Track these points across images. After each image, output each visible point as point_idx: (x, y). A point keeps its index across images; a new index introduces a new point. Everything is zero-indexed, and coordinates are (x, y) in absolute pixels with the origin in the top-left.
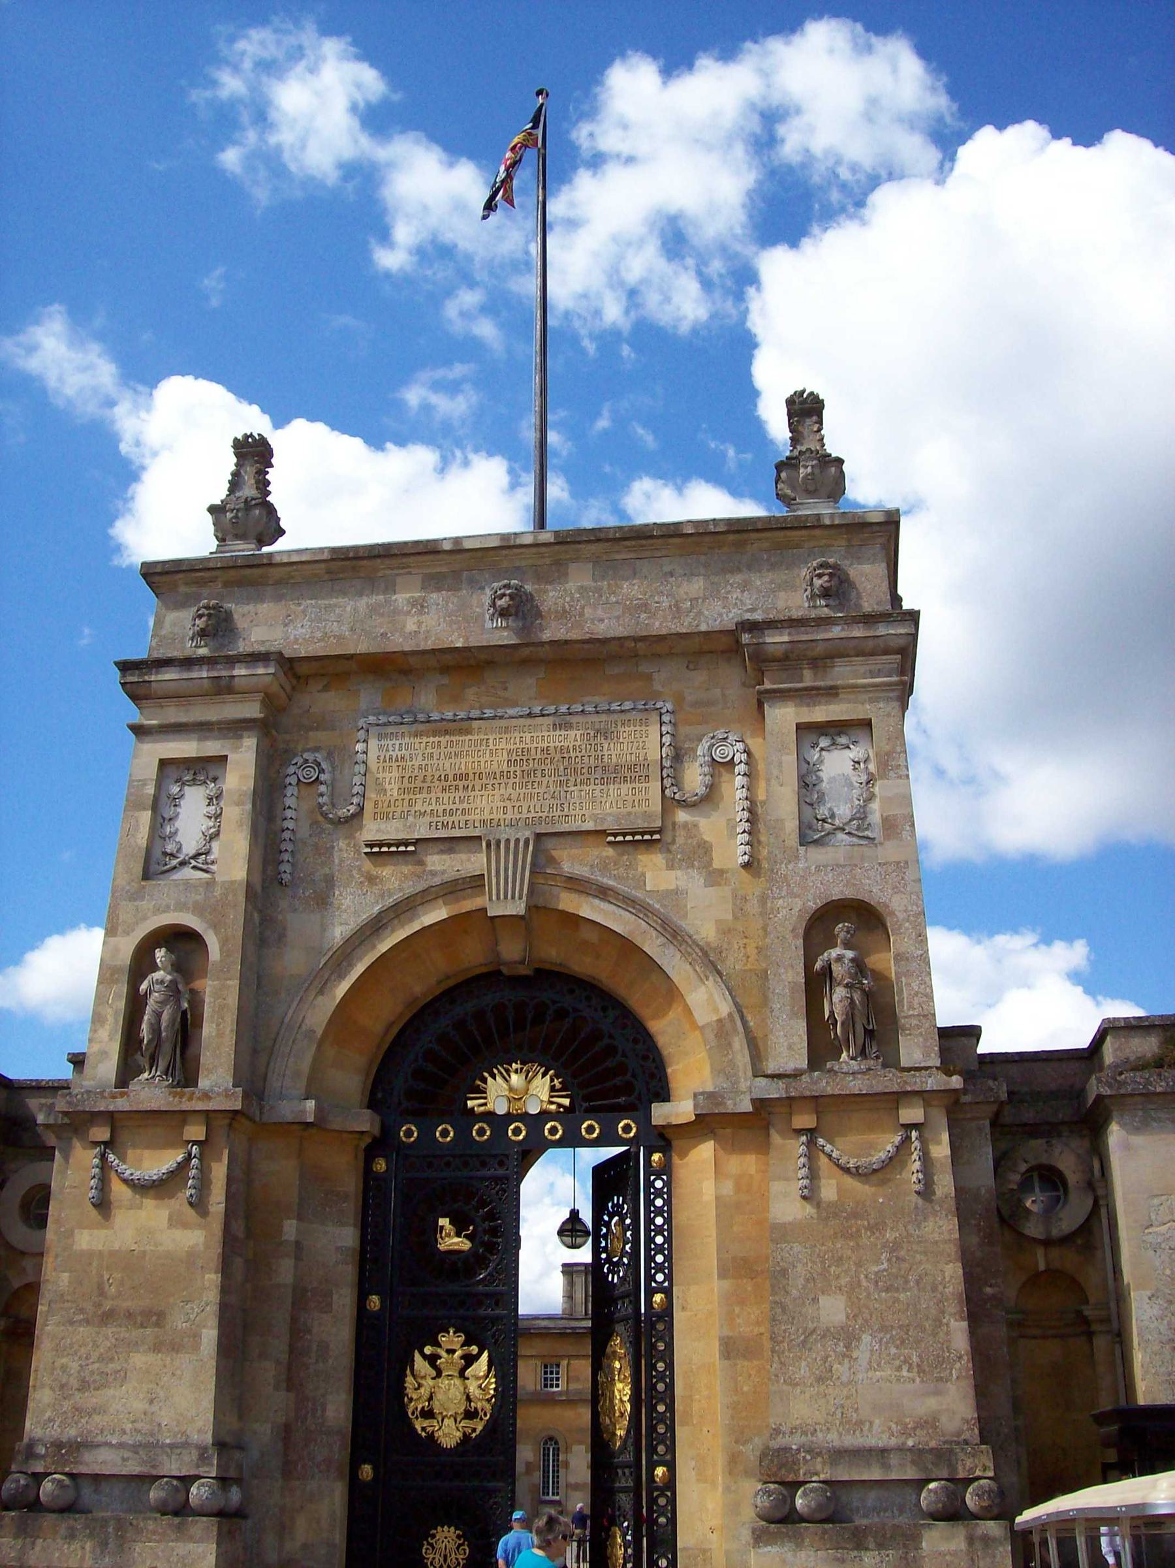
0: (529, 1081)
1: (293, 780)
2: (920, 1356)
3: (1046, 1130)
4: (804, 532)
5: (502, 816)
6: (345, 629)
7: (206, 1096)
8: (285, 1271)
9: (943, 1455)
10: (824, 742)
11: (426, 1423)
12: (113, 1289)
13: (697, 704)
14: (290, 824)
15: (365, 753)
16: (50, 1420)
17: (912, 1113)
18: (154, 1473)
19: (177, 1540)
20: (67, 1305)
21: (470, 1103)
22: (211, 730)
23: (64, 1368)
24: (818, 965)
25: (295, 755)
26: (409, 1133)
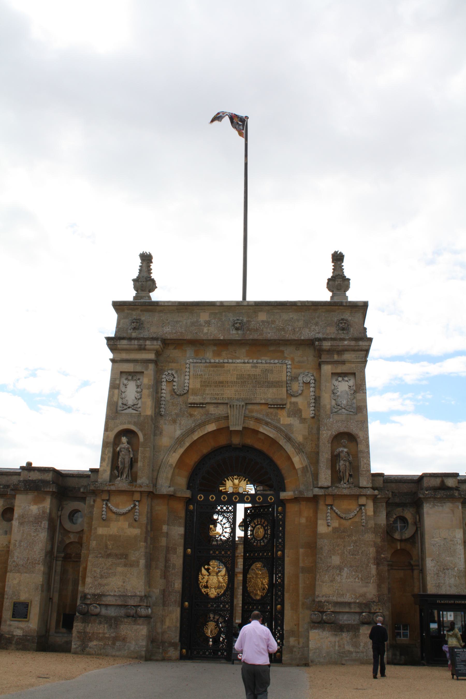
0: (240, 482)
1: (165, 380)
2: (362, 575)
3: (403, 505)
4: (337, 307)
5: (235, 397)
6: (183, 330)
7: (141, 486)
8: (163, 542)
9: (367, 605)
10: (340, 379)
11: (205, 590)
12: (110, 547)
13: (299, 362)
14: (164, 395)
15: (189, 372)
16: (91, 587)
17: (362, 501)
18: (126, 604)
19: (134, 624)
20: (95, 551)
21: (221, 488)
22: (138, 362)
23: (95, 571)
24: (335, 453)
25: (165, 371)
26: (201, 497)
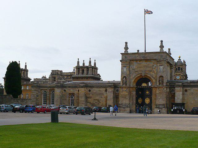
17: (164, 88)
